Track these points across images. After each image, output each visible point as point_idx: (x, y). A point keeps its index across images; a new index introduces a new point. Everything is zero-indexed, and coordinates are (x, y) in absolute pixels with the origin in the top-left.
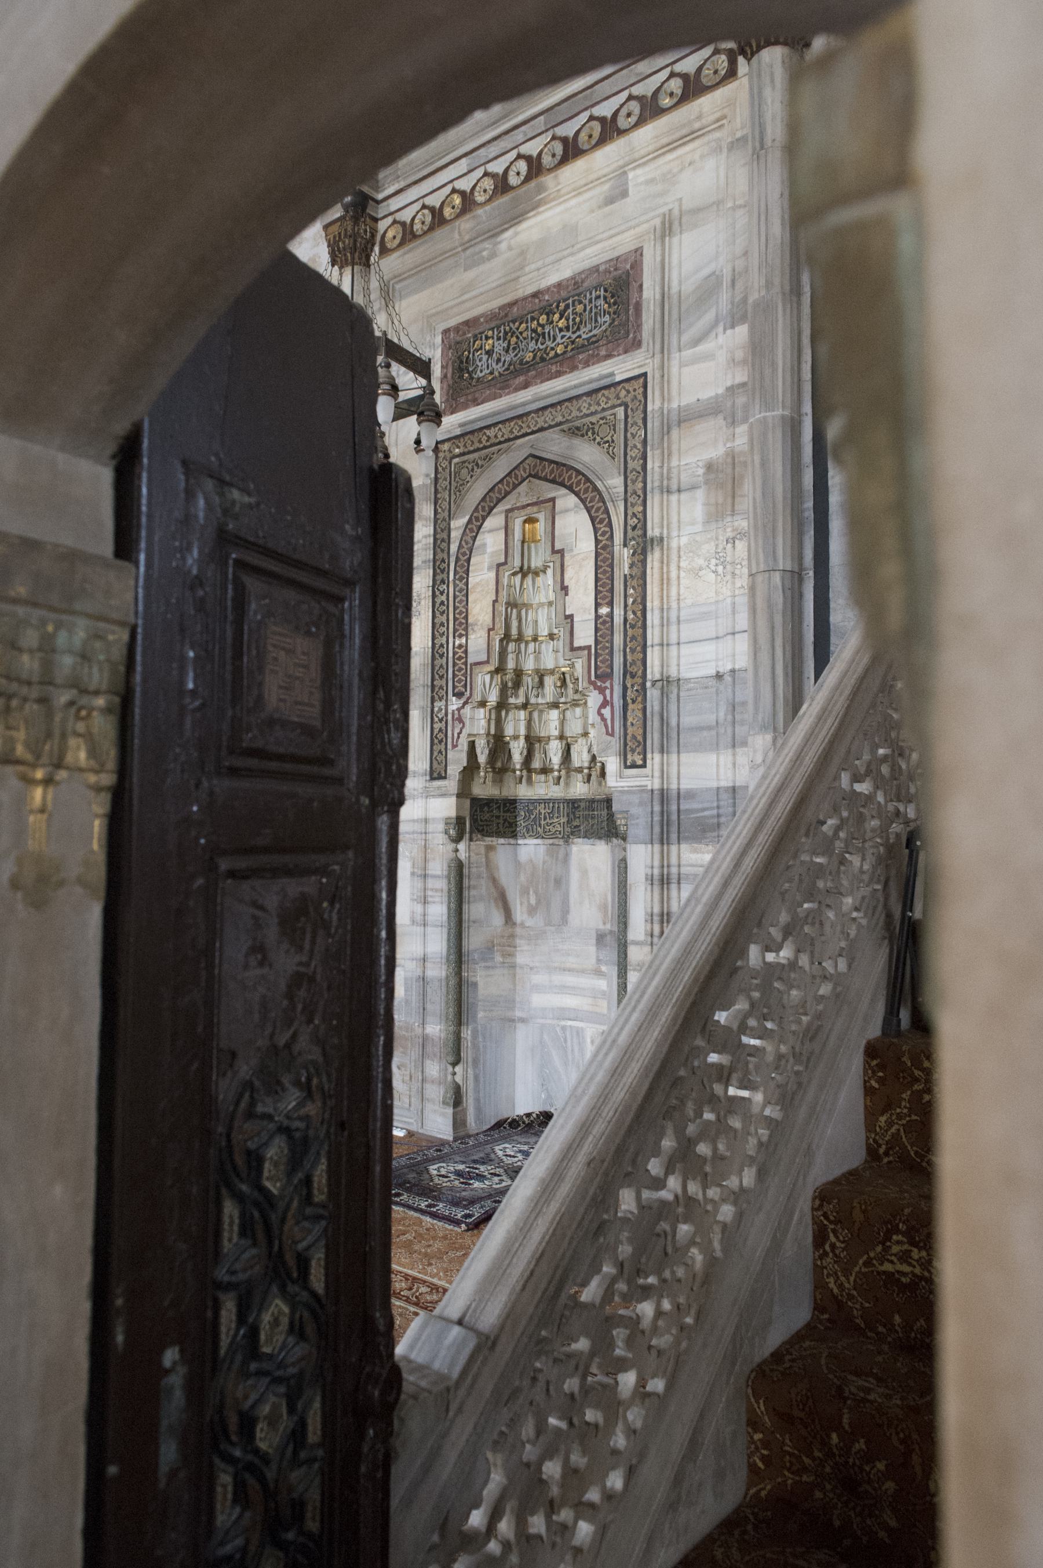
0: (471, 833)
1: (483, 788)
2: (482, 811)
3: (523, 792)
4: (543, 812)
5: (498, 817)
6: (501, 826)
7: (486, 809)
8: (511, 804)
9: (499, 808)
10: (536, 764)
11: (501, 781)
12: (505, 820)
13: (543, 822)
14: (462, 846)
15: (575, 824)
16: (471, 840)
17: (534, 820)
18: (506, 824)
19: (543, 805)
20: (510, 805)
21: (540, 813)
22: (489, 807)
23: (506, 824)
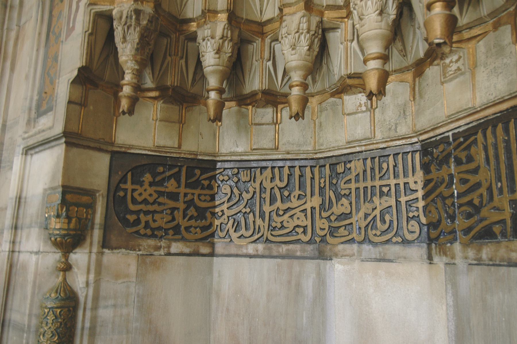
0: (106, 228)
1: (145, 131)
2: (137, 181)
3: (230, 143)
4: (268, 185)
5: (174, 196)
6: (179, 215)
7: (147, 178)
8: (204, 171)
9: (177, 176)
10: (255, 83)
11: (181, 122)
12: (190, 203)
13: (267, 208)
14: (79, 257)
15: (338, 210)
16: (105, 244)
17: (250, 203)
18: (192, 211)
19: (268, 173)
20: (201, 171)
21: (263, 190)
22: (154, 175)
23: (192, 211)
